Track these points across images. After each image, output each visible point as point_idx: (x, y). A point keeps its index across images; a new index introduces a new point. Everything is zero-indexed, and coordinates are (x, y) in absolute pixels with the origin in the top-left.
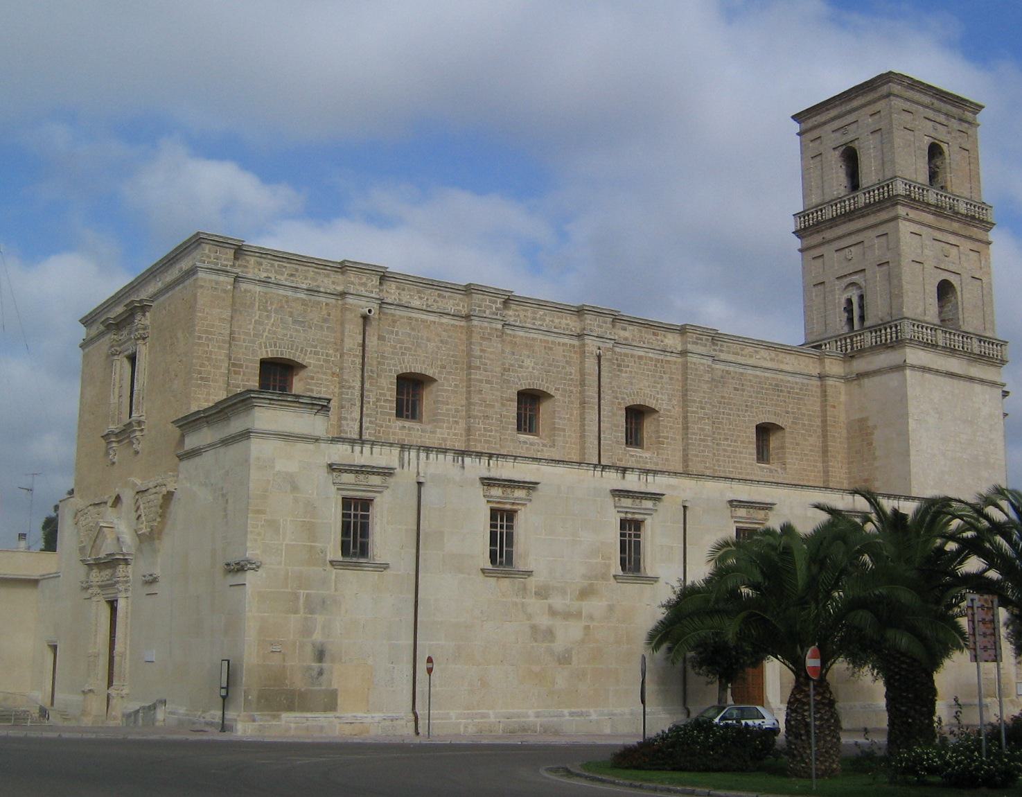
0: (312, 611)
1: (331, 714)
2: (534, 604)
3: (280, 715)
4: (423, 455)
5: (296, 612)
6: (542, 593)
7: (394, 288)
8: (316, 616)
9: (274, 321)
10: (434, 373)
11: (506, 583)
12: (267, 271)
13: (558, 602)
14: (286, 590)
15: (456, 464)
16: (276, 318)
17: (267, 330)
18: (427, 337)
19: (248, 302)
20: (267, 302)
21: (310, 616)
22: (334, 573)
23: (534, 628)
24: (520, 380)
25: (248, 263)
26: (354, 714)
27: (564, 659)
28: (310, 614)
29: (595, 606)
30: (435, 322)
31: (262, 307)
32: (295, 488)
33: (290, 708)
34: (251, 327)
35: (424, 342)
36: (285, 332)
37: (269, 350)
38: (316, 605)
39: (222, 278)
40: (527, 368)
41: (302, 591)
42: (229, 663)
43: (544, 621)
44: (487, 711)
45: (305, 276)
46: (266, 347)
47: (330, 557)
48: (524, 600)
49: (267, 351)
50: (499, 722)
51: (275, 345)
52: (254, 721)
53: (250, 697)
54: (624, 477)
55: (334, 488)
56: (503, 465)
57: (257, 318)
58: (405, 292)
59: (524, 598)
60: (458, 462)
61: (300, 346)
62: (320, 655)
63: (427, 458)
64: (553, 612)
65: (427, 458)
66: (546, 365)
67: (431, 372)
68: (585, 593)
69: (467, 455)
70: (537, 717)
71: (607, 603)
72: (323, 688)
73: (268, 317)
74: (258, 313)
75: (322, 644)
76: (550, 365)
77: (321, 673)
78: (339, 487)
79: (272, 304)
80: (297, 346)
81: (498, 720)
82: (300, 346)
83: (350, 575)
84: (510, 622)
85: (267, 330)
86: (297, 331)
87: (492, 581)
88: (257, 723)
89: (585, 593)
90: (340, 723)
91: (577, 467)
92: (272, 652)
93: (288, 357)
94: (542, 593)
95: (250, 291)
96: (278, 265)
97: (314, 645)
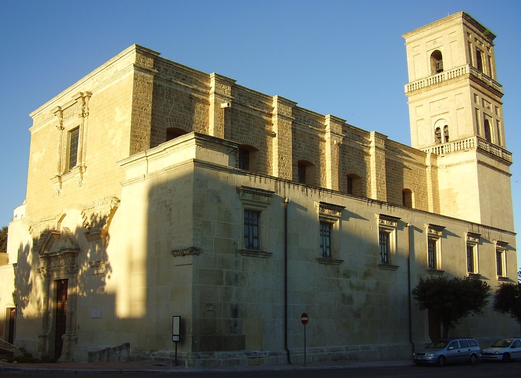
0: (230, 284)
1: (242, 352)
2: (343, 281)
3: (214, 353)
4: (287, 185)
5: (221, 284)
6: (346, 275)
7: (237, 94)
8: (232, 286)
9: (174, 105)
10: (258, 146)
11: (329, 267)
12: (170, 75)
13: (354, 280)
14: (216, 269)
15: (303, 192)
16: (176, 104)
17: (171, 111)
18: (254, 125)
19: (160, 93)
20: (170, 94)
21: (229, 286)
22: (241, 258)
23: (343, 295)
24: (299, 155)
25: (160, 69)
26: (255, 351)
27: (357, 315)
28: (229, 285)
29: (370, 282)
30: (257, 117)
31: (168, 96)
32: (219, 201)
33: (219, 349)
34: (162, 108)
35: (252, 127)
36: (181, 113)
37: (171, 123)
38: (236, 279)
39: (148, 75)
40: (302, 148)
41: (224, 270)
42: (180, 318)
43: (348, 291)
44: (322, 348)
45: (191, 81)
46: (170, 121)
47: (240, 248)
48: (338, 278)
49: (171, 124)
50: (329, 354)
51: (175, 120)
52: (199, 358)
53: (196, 342)
54: (381, 208)
55: (240, 203)
56: (326, 195)
57: (165, 103)
58: (242, 97)
59: (338, 277)
60: (304, 191)
61: (189, 123)
62: (235, 312)
63: (289, 187)
64: (352, 286)
65: (289, 187)
66: (311, 147)
67: (256, 145)
68: (366, 275)
69: (309, 187)
70: (347, 350)
71: (376, 281)
72: (237, 335)
73: (172, 103)
74: (166, 99)
75: (236, 306)
76: (313, 147)
77: (236, 325)
78: (243, 202)
79: (173, 95)
80: (187, 123)
81: (328, 353)
82: (189, 123)
83: (250, 259)
84: (332, 292)
85: (171, 111)
86: (187, 113)
87: (323, 266)
88: (201, 360)
89: (366, 275)
90: (248, 358)
91: (360, 200)
92: (208, 310)
93: (182, 128)
94: (346, 275)
95: (161, 86)
96: (176, 72)
97: (231, 305)
